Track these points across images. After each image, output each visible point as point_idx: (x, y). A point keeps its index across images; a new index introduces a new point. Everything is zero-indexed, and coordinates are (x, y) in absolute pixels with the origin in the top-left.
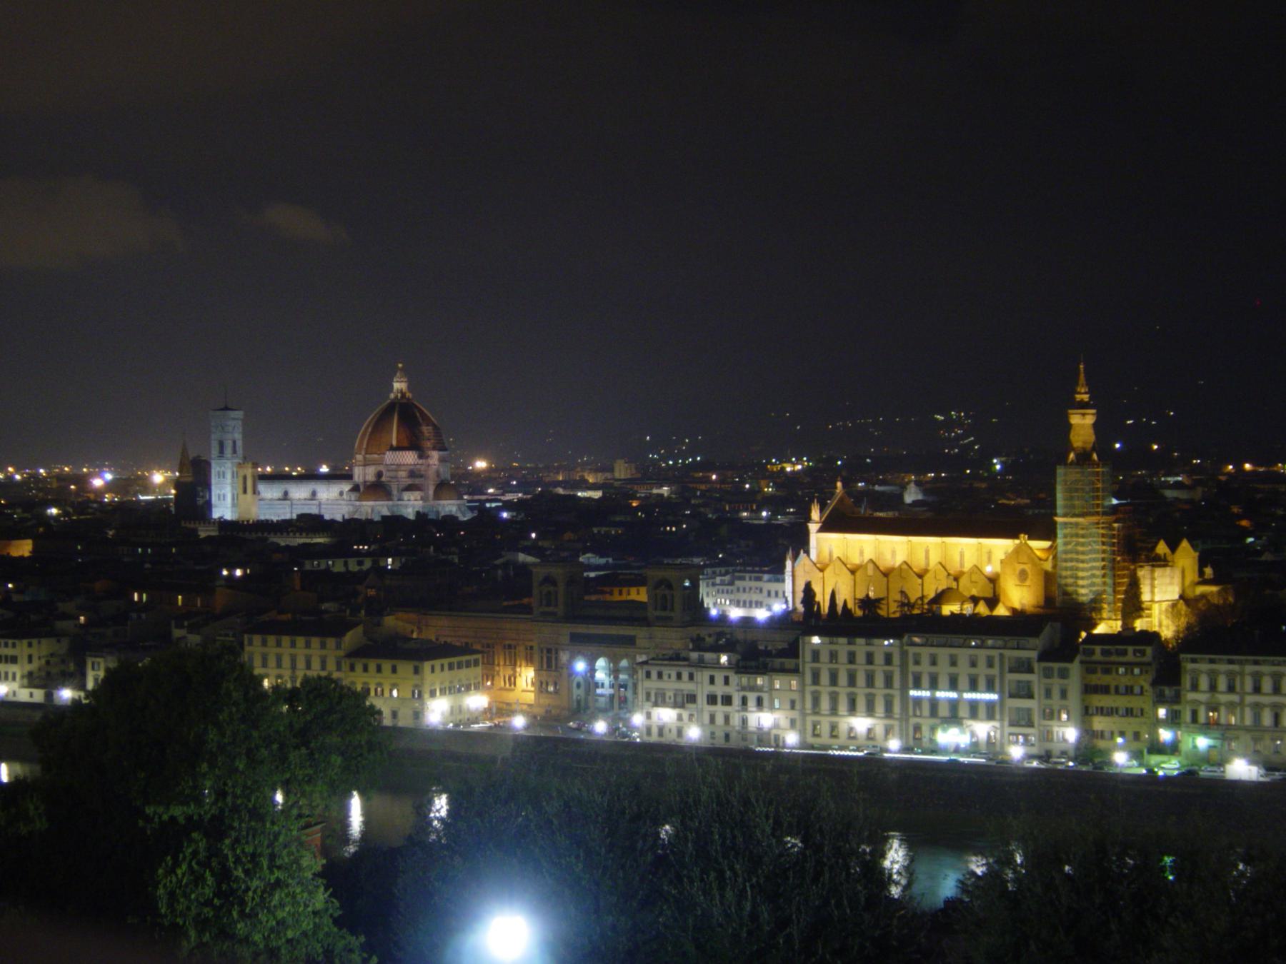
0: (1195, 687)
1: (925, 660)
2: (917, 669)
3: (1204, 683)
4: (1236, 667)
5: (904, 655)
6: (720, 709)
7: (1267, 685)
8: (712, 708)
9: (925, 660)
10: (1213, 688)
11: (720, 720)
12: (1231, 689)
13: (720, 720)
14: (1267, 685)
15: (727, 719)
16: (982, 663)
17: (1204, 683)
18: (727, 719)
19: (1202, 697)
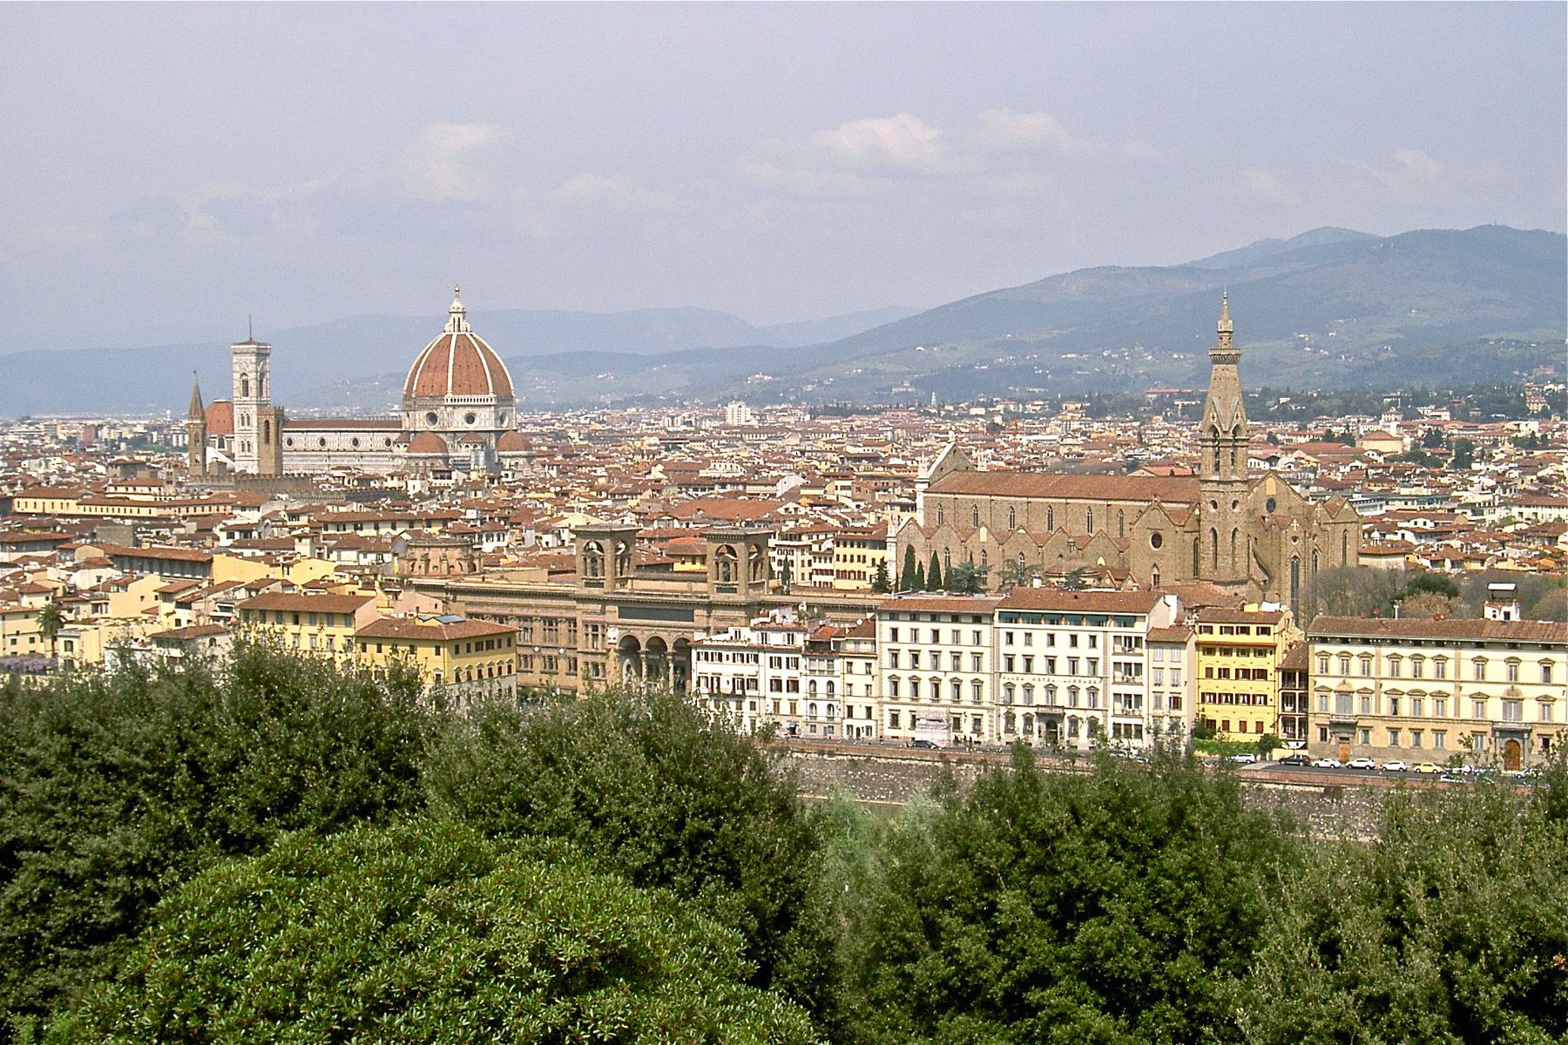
0: (1325, 669)
2: (1010, 650)
3: (1335, 665)
4: (1371, 649)
6: (785, 696)
7: (1406, 668)
8: (777, 695)
9: (1019, 637)
10: (1346, 669)
11: (785, 708)
12: (1366, 672)
13: (785, 708)
14: (1406, 668)
15: (793, 707)
16: (1083, 639)
17: (1335, 665)
18: (793, 707)
19: (1333, 684)
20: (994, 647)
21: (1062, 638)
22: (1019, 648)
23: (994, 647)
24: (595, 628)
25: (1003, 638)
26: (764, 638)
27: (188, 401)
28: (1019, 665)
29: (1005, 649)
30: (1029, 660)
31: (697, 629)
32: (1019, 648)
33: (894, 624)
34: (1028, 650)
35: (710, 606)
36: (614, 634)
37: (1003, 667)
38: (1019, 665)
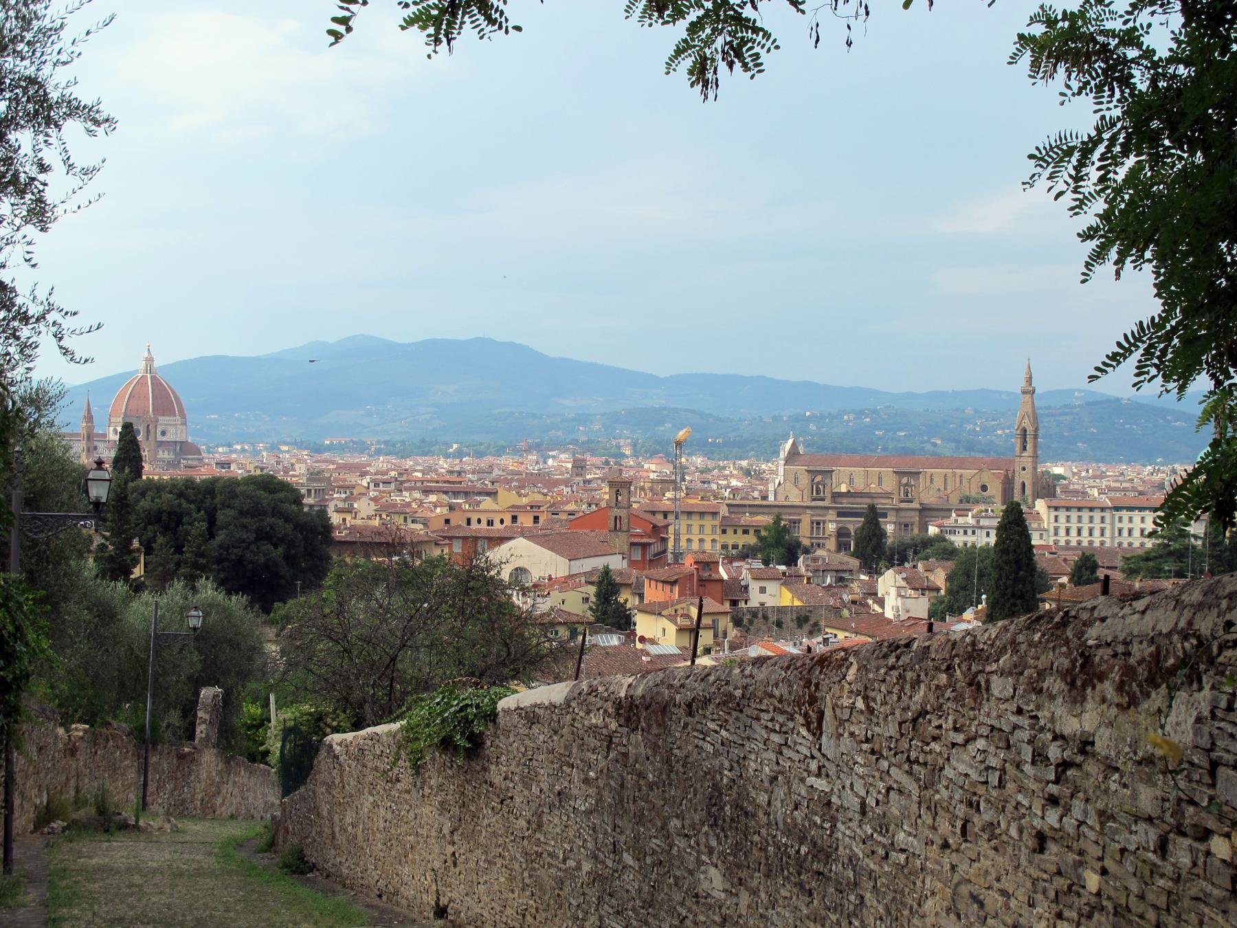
1: (1125, 519)
2: (1120, 525)
5: (1113, 516)
9: (1125, 519)
20: (1113, 524)
21: (1137, 519)
22: (1125, 525)
23: (1113, 524)
24: (818, 523)
25: (1117, 519)
26: (978, 522)
27: (84, 413)
28: (1125, 533)
29: (1118, 525)
30: (1130, 531)
31: (890, 522)
32: (1125, 525)
33: (1056, 513)
34: (1131, 526)
35: (898, 510)
36: (832, 527)
37: (1116, 534)
38: (1125, 533)
